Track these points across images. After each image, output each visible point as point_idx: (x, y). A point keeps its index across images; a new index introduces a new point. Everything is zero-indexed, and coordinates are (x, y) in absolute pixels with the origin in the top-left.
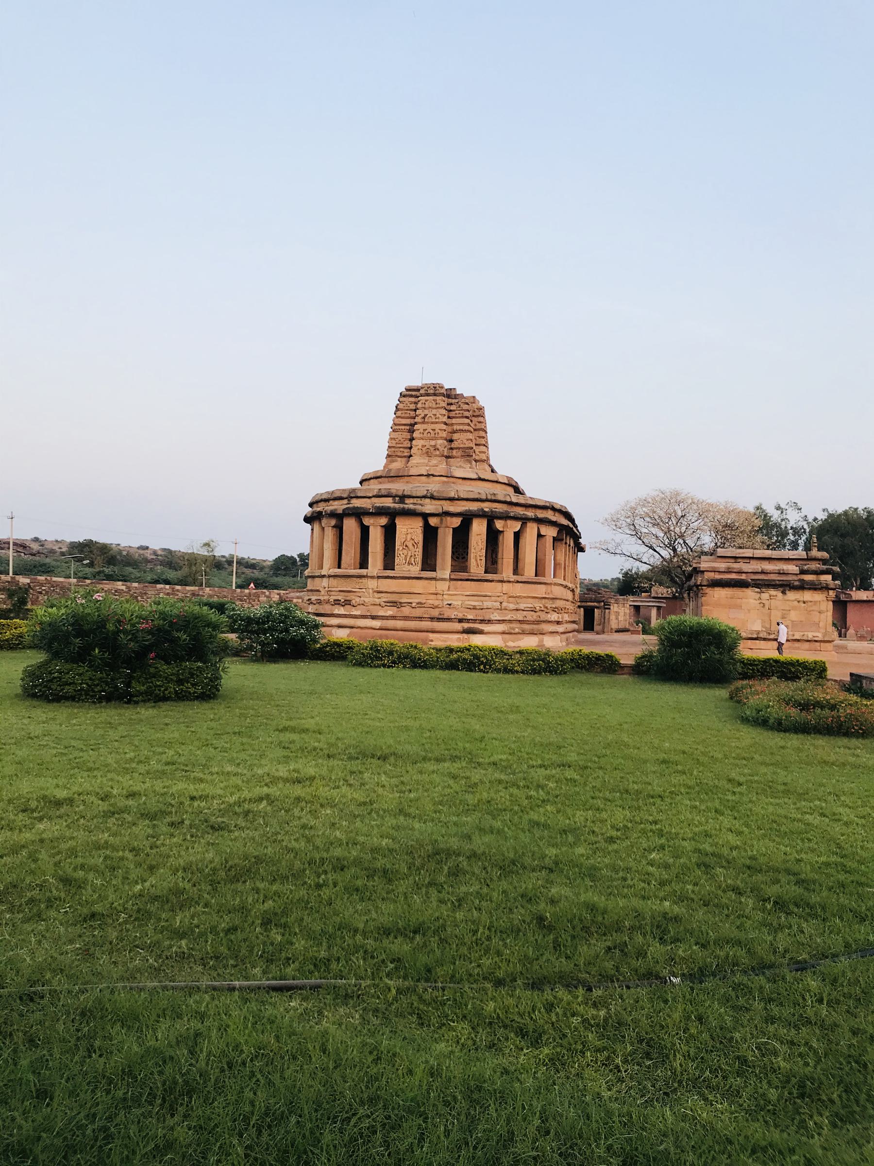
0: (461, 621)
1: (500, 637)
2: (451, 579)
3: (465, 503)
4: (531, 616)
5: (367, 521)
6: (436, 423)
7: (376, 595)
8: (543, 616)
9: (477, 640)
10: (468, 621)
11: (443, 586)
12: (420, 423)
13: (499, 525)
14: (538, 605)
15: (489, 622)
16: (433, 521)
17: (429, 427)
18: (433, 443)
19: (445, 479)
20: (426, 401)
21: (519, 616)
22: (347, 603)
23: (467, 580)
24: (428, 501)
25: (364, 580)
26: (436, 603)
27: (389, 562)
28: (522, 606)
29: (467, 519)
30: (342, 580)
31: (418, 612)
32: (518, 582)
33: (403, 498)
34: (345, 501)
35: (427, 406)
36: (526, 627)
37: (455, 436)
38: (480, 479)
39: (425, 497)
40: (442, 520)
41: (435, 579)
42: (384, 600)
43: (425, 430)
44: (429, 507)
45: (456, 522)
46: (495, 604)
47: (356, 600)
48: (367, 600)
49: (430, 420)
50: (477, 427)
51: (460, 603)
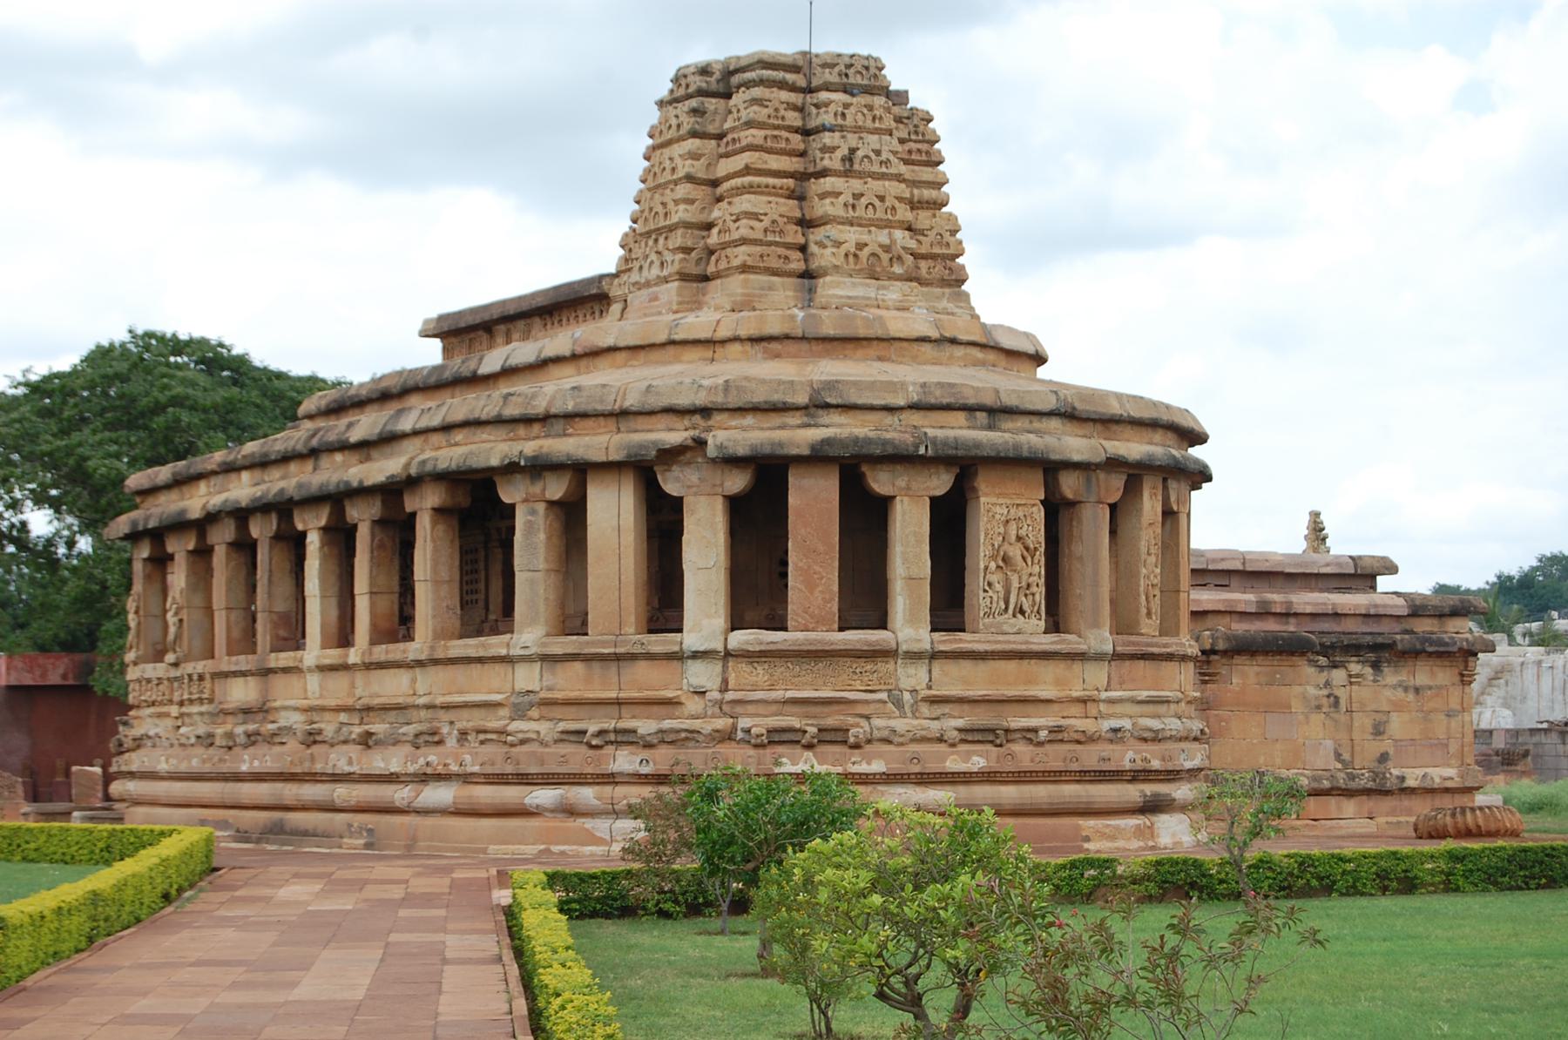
2: (1117, 657)
5: (880, 482)
6: (883, 177)
7: (925, 709)
11: (1096, 676)
12: (836, 174)
16: (1069, 485)
17: (876, 186)
18: (883, 237)
19: (978, 354)
20: (847, 106)
22: (833, 737)
24: (1054, 424)
25: (884, 667)
27: (949, 603)
30: (780, 670)
31: (1054, 758)
33: (998, 412)
34: (794, 419)
35: (849, 121)
39: (1051, 414)
40: (1088, 480)
41: (1081, 657)
42: (960, 723)
43: (858, 196)
44: (1075, 445)
47: (859, 731)
48: (900, 725)
49: (866, 166)
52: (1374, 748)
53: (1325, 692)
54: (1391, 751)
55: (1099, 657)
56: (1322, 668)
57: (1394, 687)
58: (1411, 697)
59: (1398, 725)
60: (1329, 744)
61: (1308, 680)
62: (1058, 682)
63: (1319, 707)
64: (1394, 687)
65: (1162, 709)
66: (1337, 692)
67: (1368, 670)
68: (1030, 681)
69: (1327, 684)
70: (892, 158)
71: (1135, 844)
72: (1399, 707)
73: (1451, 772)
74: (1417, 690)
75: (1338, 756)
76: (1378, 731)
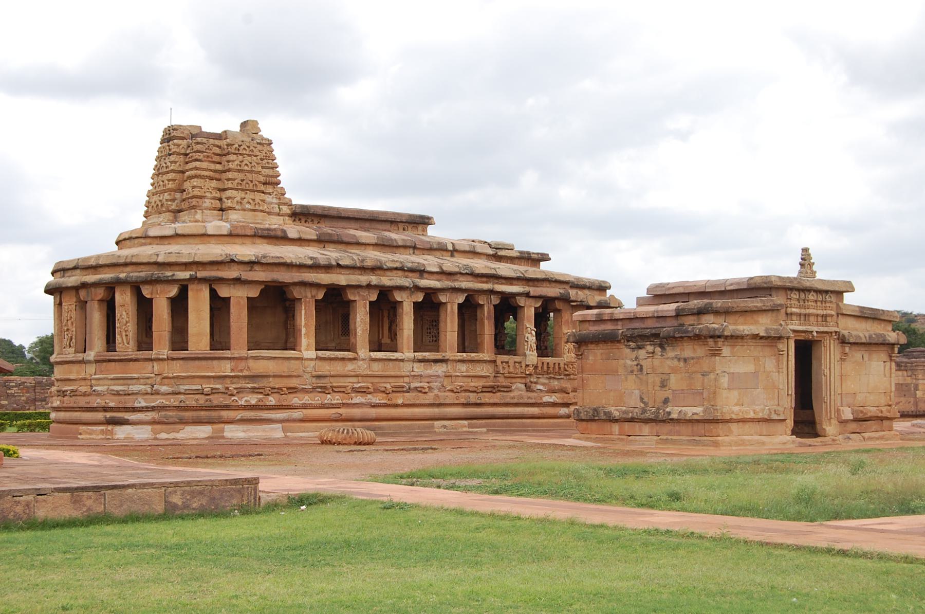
0: (106, 409)
1: (149, 427)
3: (107, 269)
4: (191, 401)
6: (168, 172)
8: (217, 400)
9: (121, 432)
10: (111, 409)
11: (91, 369)
13: (146, 292)
14: (207, 387)
15: (134, 410)
19: (143, 241)
21: (174, 401)
23: (110, 361)
26: (83, 389)
28: (182, 388)
29: (111, 287)
32: (173, 359)
36: (188, 414)
37: (187, 185)
38: (177, 236)
45: (100, 293)
46: (142, 387)
50: (226, 168)
51: (106, 387)
52: (662, 395)
53: (635, 363)
54: (671, 397)
55: (89, 362)
56: (633, 349)
57: (672, 359)
58: (682, 364)
59: (674, 381)
60: (637, 392)
61: (627, 356)
62: (78, 373)
63: (632, 372)
64: (672, 359)
65: (129, 382)
66: (641, 363)
67: (658, 349)
68: (70, 372)
69: (636, 358)
70: (169, 164)
71: (101, 436)
72: (674, 370)
73: (699, 410)
74: (685, 360)
75: (642, 399)
76: (663, 385)
